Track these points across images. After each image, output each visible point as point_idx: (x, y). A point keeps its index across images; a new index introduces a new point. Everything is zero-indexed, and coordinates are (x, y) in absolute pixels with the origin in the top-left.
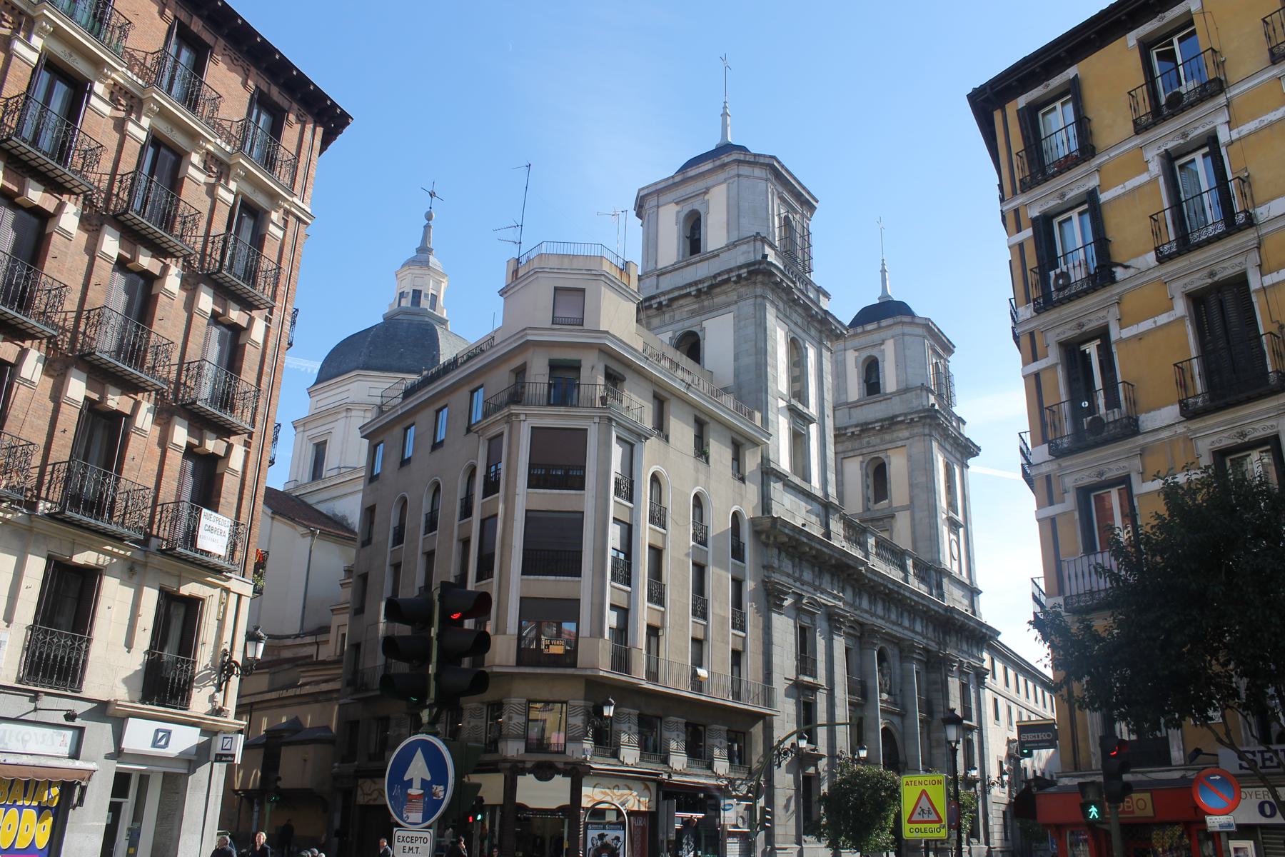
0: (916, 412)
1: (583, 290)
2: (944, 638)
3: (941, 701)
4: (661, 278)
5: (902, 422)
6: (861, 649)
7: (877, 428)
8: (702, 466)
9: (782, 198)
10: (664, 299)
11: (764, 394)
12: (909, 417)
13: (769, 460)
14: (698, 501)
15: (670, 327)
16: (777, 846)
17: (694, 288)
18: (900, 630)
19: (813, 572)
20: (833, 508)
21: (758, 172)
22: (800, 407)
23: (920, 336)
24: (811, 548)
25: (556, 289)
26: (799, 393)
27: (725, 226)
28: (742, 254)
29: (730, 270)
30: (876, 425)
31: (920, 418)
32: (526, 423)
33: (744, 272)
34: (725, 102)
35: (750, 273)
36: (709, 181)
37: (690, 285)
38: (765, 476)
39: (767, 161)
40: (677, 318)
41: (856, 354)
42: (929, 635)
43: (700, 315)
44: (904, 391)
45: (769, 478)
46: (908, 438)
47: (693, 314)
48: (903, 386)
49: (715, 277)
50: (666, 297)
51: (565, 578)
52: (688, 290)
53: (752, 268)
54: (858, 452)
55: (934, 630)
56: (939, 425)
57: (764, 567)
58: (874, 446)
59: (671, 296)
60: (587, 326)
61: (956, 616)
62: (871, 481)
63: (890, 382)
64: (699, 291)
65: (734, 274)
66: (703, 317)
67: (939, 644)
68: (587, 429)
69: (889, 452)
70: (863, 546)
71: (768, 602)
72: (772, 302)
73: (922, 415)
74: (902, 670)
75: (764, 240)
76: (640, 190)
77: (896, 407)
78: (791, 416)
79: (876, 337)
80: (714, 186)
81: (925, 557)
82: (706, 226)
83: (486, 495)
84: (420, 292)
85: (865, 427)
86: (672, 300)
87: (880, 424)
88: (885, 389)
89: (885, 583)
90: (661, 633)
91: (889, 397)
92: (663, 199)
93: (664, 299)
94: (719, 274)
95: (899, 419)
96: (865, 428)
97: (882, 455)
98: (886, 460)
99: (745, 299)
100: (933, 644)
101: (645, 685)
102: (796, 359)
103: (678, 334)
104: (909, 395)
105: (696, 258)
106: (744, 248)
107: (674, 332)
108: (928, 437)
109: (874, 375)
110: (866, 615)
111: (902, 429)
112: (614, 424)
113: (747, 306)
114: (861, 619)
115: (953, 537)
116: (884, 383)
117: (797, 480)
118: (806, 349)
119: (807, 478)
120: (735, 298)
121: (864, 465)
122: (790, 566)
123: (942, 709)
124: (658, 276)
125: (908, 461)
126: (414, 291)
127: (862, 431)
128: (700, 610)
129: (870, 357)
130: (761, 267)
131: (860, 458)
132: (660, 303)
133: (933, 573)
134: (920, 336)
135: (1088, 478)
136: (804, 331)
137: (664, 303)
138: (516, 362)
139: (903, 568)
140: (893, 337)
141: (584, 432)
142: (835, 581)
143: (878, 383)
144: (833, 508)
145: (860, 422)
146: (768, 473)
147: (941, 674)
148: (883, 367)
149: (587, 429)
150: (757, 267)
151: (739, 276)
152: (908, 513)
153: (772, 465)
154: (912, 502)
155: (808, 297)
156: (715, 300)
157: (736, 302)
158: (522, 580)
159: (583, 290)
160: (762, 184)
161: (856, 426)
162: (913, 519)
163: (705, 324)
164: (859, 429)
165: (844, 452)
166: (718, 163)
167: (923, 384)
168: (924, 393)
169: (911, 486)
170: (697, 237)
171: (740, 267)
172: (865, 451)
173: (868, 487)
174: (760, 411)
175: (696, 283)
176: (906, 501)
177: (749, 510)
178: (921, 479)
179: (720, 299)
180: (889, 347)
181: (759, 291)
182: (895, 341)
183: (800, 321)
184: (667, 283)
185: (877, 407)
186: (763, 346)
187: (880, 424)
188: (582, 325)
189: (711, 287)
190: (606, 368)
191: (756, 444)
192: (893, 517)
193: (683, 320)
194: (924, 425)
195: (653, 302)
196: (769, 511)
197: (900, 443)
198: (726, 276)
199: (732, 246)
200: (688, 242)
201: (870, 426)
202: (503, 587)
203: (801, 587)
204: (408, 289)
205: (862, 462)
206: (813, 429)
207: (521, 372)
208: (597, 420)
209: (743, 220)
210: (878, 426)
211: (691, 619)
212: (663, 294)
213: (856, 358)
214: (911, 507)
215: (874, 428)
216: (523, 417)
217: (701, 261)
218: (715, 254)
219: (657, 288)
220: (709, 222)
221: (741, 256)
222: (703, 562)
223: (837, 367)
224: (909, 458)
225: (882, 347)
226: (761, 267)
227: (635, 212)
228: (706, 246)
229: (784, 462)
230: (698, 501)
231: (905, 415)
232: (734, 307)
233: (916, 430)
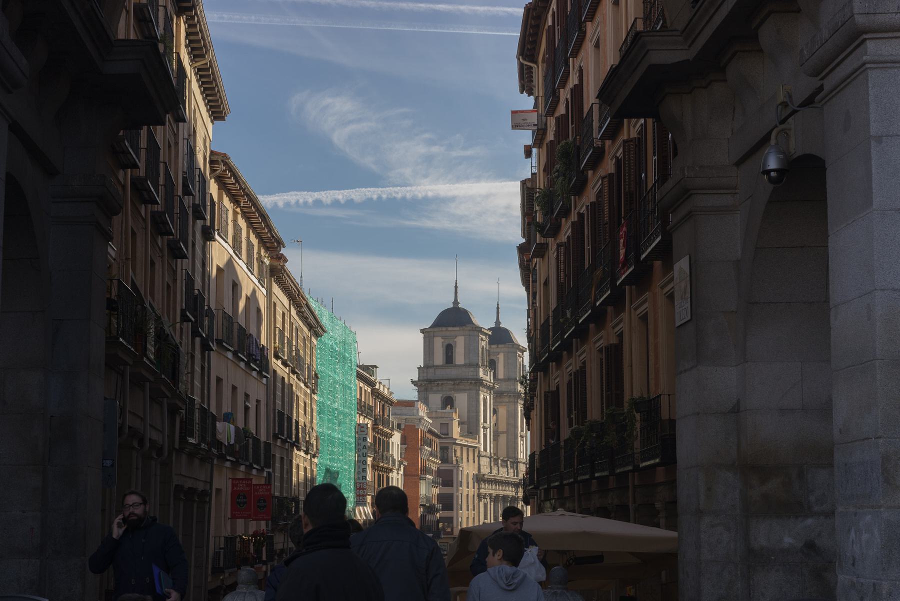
25: (441, 423)
28: (471, 371)
50: (441, 382)
59: (443, 382)
80: (459, 336)
103: (444, 396)
107: (443, 395)
141: (452, 471)
151: (471, 383)
152: (505, 435)
156: (460, 387)
159: (448, 424)
166: (461, 328)
170: (450, 354)
176: (505, 430)
180: (501, 357)
182: (504, 355)
188: (448, 435)
195: (435, 383)
197: (503, 404)
199: (465, 365)
206: (488, 430)
214: (507, 432)
218: (460, 366)
220: (457, 350)
224: (508, 411)
225: (498, 356)
233: (511, 400)
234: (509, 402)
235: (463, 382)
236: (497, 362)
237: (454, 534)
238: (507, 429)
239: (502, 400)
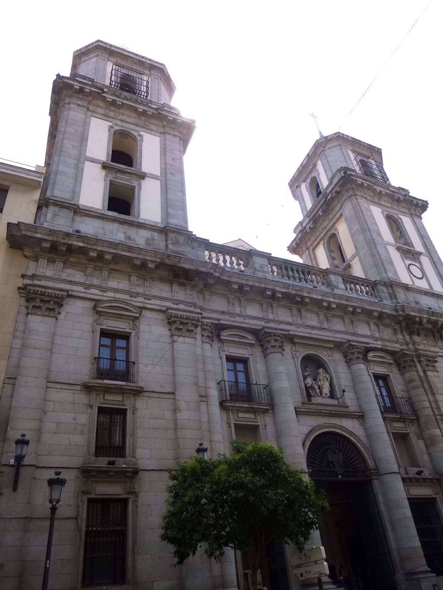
3: (425, 397)
7: (321, 214)
12: (334, 191)
19: (129, 280)
23: (336, 146)
30: (319, 212)
31: (341, 186)
58: (325, 227)
69: (336, 226)
85: (314, 219)
87: (321, 210)
89: (271, 287)
95: (329, 197)
97: (333, 231)
115: (408, 262)
121: (326, 245)
123: (427, 404)
125: (346, 222)
131: (322, 242)
134: (336, 146)
147: (417, 371)
148: (319, 178)
154: (356, 248)
162: (360, 259)
164: (311, 222)
165: (312, 244)
172: (322, 235)
176: (354, 251)
187: (321, 210)
203: (101, 293)
205: (324, 244)
210: (320, 213)
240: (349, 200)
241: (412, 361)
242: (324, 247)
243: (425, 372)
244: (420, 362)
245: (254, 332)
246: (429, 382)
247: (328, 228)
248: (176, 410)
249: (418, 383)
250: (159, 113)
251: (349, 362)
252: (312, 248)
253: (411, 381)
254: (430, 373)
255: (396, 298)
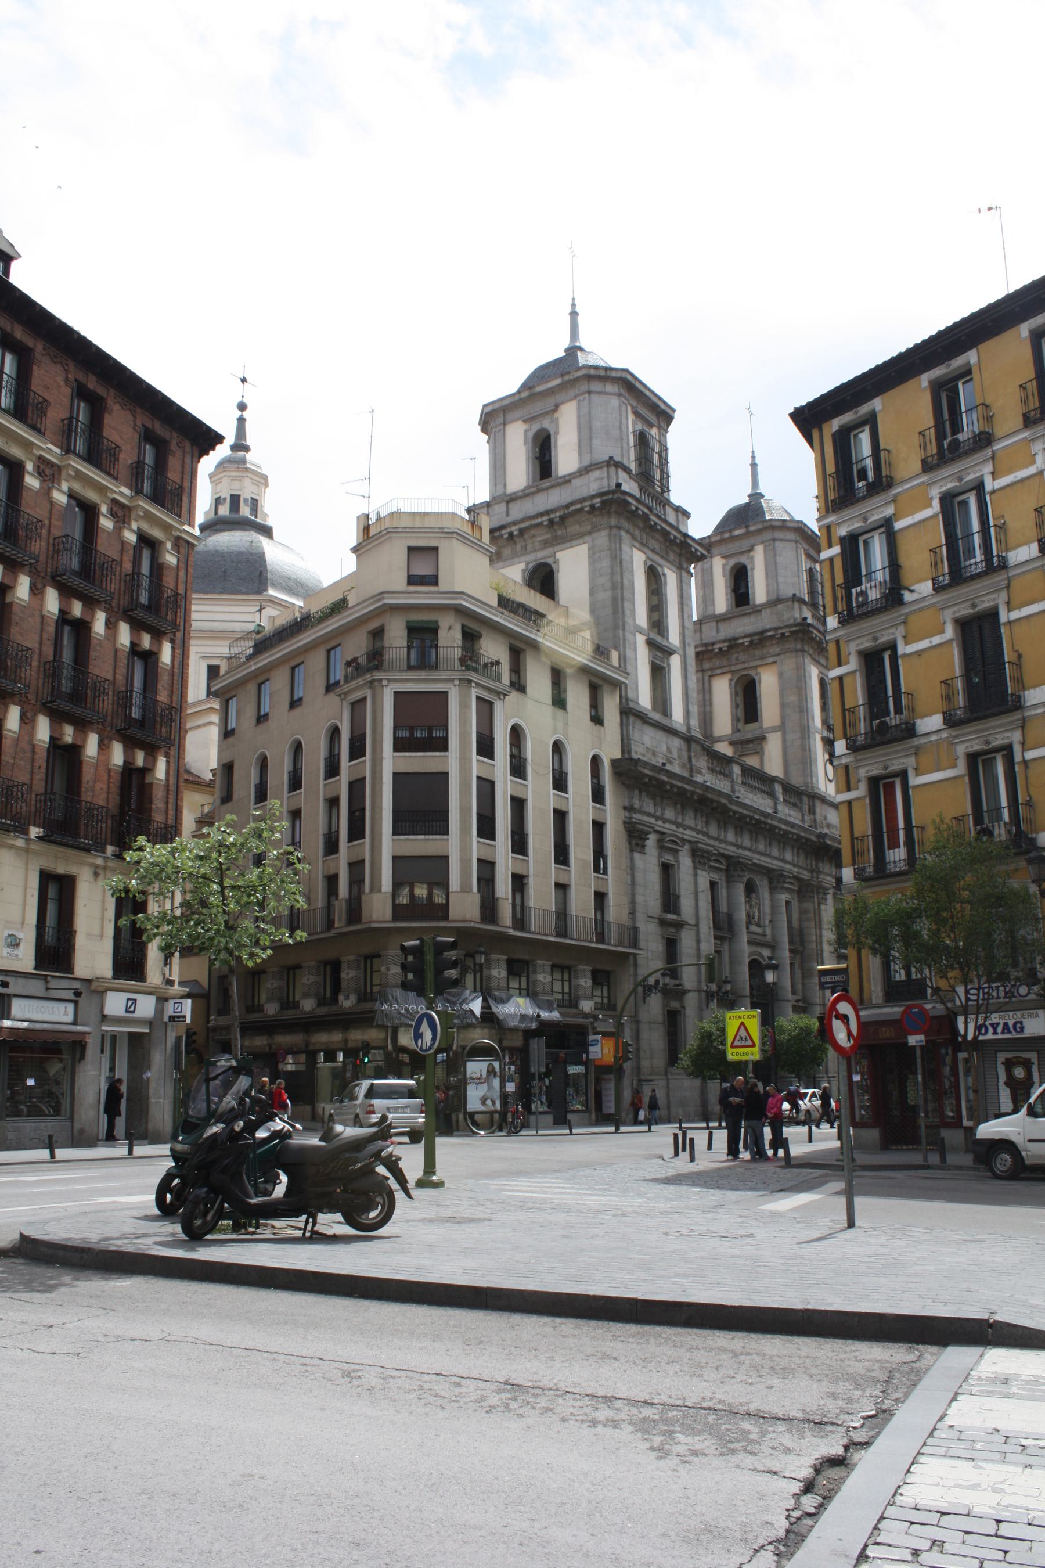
0: (786, 627)
1: (435, 549)
2: (816, 865)
3: (813, 931)
4: (511, 505)
5: (772, 637)
6: (728, 882)
8: (560, 712)
9: (636, 413)
10: (515, 529)
11: (621, 632)
12: (780, 631)
13: (627, 700)
14: (558, 748)
15: (522, 559)
16: (643, 1078)
17: (545, 518)
18: (768, 860)
19: (675, 808)
20: (695, 741)
21: (610, 388)
22: (659, 639)
24: (673, 786)
25: (410, 549)
26: (658, 624)
27: (576, 448)
28: (596, 480)
29: (583, 500)
31: (792, 632)
32: (389, 688)
33: (597, 501)
34: (573, 299)
35: (602, 502)
36: (559, 398)
37: (542, 514)
38: (624, 718)
39: (619, 375)
40: (529, 547)
41: (724, 561)
42: (800, 864)
43: (553, 545)
44: (775, 602)
45: (628, 718)
46: (779, 655)
47: (546, 544)
48: (774, 597)
49: (567, 506)
50: (517, 527)
51: (434, 837)
52: (540, 520)
53: (605, 498)
54: (724, 670)
55: (806, 858)
56: (813, 639)
57: (625, 808)
58: (744, 662)
59: (523, 525)
60: (443, 585)
61: (829, 842)
62: (740, 700)
63: (760, 593)
64: (551, 522)
65: (588, 503)
66: (556, 548)
67: (811, 871)
68: (447, 693)
69: (760, 670)
70: (728, 775)
71: (630, 843)
72: (627, 532)
73: (794, 629)
74: (772, 900)
75: (618, 465)
76: (485, 406)
77: (766, 621)
78: (650, 650)
79: (745, 544)
80: (563, 403)
81: (796, 781)
82: (556, 447)
83: (352, 757)
84: (238, 496)
86: (522, 532)
88: (754, 599)
89: (751, 814)
90: (526, 881)
91: (758, 610)
92: (509, 416)
93: (515, 529)
94: (572, 504)
95: (769, 634)
96: (733, 644)
97: (752, 673)
98: (756, 678)
99: (599, 530)
100: (805, 872)
101: (512, 932)
102: (654, 586)
103: (531, 566)
104: (780, 606)
105: (546, 483)
106: (597, 474)
107: (527, 564)
108: (800, 654)
109: (743, 584)
110: (731, 848)
111: (772, 645)
112: (473, 685)
113: (602, 538)
114: (726, 852)
116: (754, 593)
117: (656, 716)
118: (664, 575)
119: (666, 712)
120: (589, 528)
121: (733, 682)
122: (651, 805)
124: (508, 502)
126: (232, 496)
127: (730, 647)
128: (562, 855)
129: (736, 565)
130: (616, 496)
131: (729, 676)
132: (511, 534)
133: (805, 799)
135: (876, 771)
136: (662, 557)
137: (515, 533)
138: (374, 625)
139: (772, 795)
140: (762, 543)
141: (445, 694)
142: (699, 816)
143: (747, 594)
144: (695, 741)
145: (729, 636)
146: (629, 712)
149: (447, 693)
150: (610, 496)
151: (592, 507)
152: (779, 734)
153: (632, 705)
154: (783, 723)
155: (665, 521)
157: (590, 533)
158: (393, 840)
159: (435, 549)
160: (615, 402)
161: (724, 641)
162: (784, 741)
163: (559, 555)
164: (726, 644)
165: (711, 669)
167: (794, 595)
168: (796, 605)
169: (783, 706)
170: (547, 458)
171: (593, 497)
172: (733, 668)
173: (737, 706)
174: (616, 648)
175: (547, 512)
177: (611, 752)
178: (793, 698)
179: (574, 529)
181: (613, 521)
182: (765, 547)
183: (657, 546)
184: (518, 511)
185: (746, 620)
186: (619, 579)
189: (563, 518)
190: (463, 626)
191: (615, 684)
192: (763, 738)
193: (535, 551)
194: (796, 640)
195: (503, 532)
196: (629, 752)
197: (771, 660)
198: (578, 506)
199: (585, 471)
200: (537, 462)
201: (740, 641)
202: (376, 849)
204: (226, 494)
205: (731, 680)
207: (378, 634)
208: (457, 682)
209: (596, 442)
211: (553, 865)
212: (514, 523)
213: (724, 566)
214: (782, 728)
215: (743, 643)
216: (385, 683)
217: (552, 487)
218: (567, 480)
219: (508, 514)
221: (594, 484)
222: (564, 809)
223: (703, 576)
224: (781, 675)
225: (752, 554)
226: (616, 496)
227: (479, 428)
228: (557, 470)
229: (644, 699)
230: (558, 748)
231: (776, 629)
232: (587, 538)
234: (784, 652)
235: (572, 508)
236: (749, 567)
237: (451, 917)
238: (783, 717)
239: (765, 651)
240: (794, 654)
241: (813, 891)
242: (730, 685)
243: (819, 904)
244: (818, 893)
245: (728, 858)
246: (820, 916)
247: (746, 665)
248: (698, 941)
249: (812, 915)
250: (686, 542)
251: (773, 890)
252: (710, 673)
253: (806, 912)
254: (823, 907)
255: (814, 813)
